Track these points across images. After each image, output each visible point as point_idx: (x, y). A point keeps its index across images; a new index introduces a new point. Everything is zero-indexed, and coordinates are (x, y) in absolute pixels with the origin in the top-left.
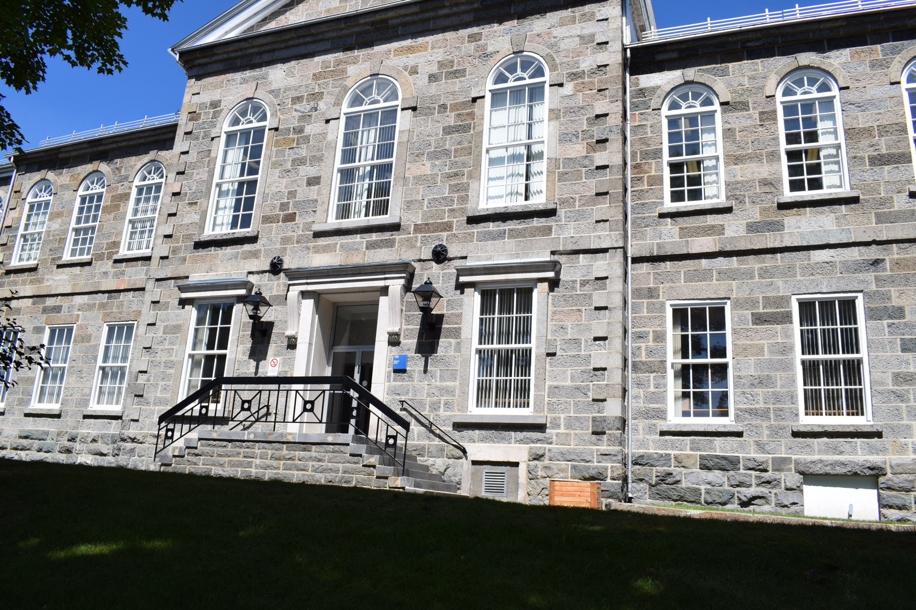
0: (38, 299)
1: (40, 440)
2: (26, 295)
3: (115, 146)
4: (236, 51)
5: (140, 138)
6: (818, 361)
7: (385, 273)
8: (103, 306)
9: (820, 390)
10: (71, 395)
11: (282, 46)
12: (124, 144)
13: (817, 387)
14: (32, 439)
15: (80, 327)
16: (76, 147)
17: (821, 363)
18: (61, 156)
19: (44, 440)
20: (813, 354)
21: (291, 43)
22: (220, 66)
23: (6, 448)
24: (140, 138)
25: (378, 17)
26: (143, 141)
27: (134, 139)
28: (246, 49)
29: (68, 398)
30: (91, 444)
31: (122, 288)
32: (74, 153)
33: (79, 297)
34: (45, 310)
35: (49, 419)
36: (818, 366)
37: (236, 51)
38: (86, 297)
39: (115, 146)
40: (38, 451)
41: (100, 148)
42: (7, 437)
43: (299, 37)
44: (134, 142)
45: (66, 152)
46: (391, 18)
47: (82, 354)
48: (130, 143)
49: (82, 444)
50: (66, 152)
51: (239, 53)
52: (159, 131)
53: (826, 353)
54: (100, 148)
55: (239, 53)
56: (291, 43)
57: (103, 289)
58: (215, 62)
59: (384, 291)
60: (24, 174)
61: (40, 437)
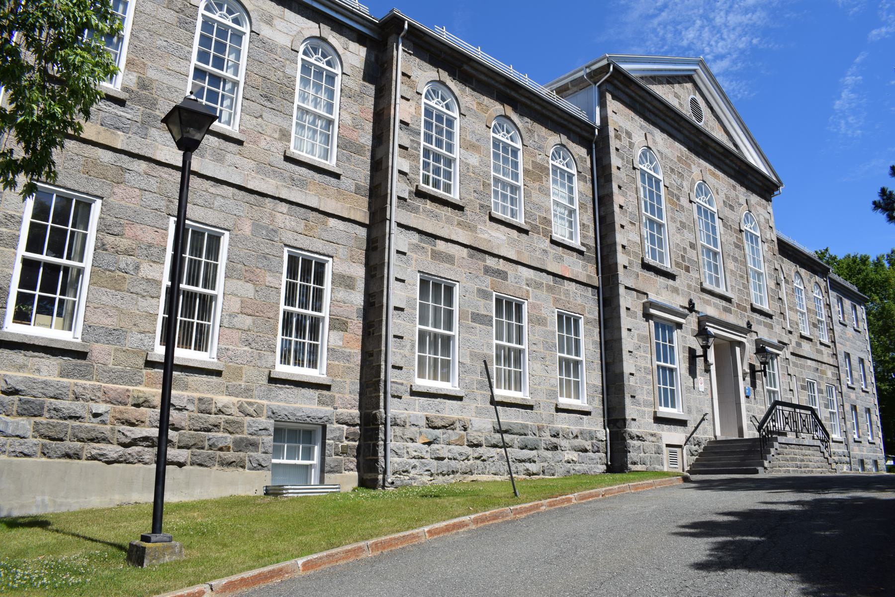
0: (475, 252)
1: (521, 435)
2: (460, 241)
3: (529, 102)
4: (640, 96)
5: (554, 113)
6: (196, 294)
7: (741, 333)
8: (550, 289)
9: (193, 323)
10: (539, 384)
11: (663, 117)
12: (538, 107)
13: (191, 320)
14: (512, 434)
15: (533, 306)
16: (491, 74)
17: (198, 296)
18: (465, 67)
19: (525, 435)
20: (193, 285)
21: (668, 119)
22: (627, 100)
23: (481, 446)
24: (554, 113)
25: (709, 142)
26: (555, 117)
27: (548, 110)
28: (646, 101)
29: (536, 386)
30: (573, 441)
31: (567, 275)
32: (483, 77)
33: (525, 269)
34: (487, 270)
35: (521, 410)
36: (292, 317)
37: (640, 96)
38: (532, 271)
39: (529, 102)
40: (522, 449)
41: (513, 94)
42: (479, 431)
43: (673, 120)
44: (547, 113)
45: (476, 70)
46: (711, 147)
47: (542, 339)
48: (544, 111)
49: (565, 440)
50: (472, 67)
51: (641, 100)
52: (573, 121)
53: (189, 284)
54: (513, 94)
55: (641, 100)
56: (668, 119)
57: (549, 269)
58: (624, 92)
59: (679, 326)
60: (410, 54)
61: (522, 431)
